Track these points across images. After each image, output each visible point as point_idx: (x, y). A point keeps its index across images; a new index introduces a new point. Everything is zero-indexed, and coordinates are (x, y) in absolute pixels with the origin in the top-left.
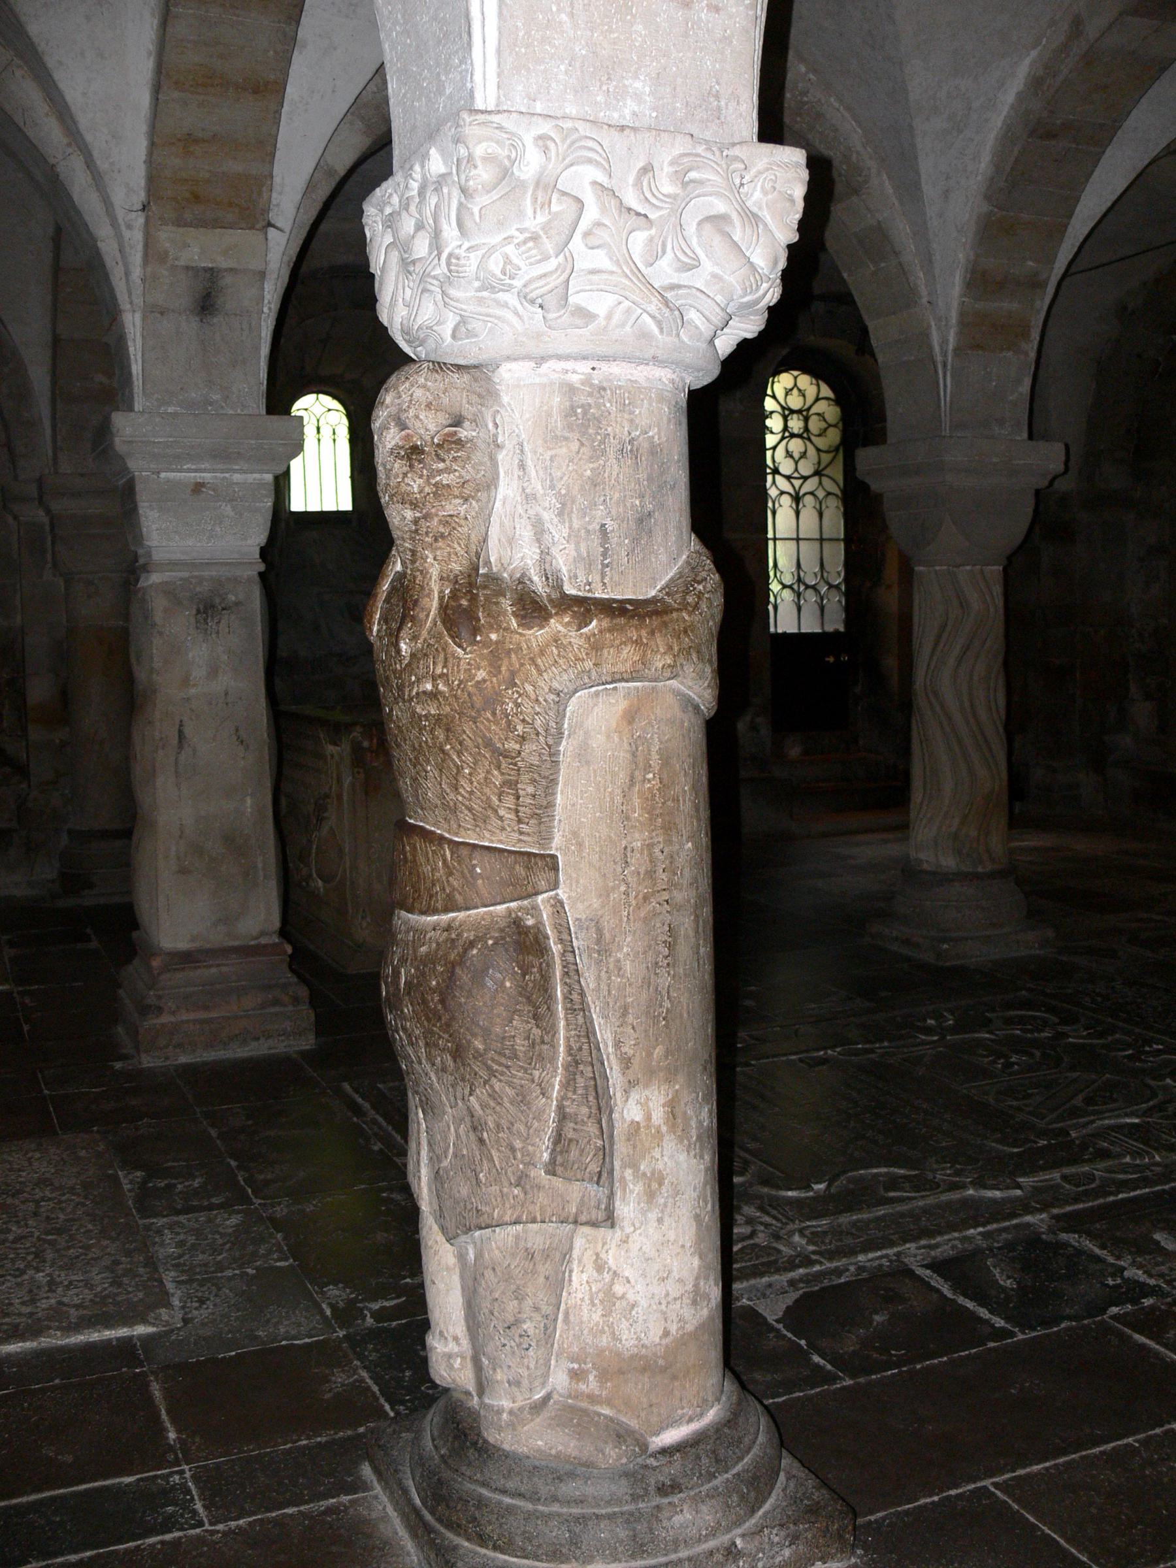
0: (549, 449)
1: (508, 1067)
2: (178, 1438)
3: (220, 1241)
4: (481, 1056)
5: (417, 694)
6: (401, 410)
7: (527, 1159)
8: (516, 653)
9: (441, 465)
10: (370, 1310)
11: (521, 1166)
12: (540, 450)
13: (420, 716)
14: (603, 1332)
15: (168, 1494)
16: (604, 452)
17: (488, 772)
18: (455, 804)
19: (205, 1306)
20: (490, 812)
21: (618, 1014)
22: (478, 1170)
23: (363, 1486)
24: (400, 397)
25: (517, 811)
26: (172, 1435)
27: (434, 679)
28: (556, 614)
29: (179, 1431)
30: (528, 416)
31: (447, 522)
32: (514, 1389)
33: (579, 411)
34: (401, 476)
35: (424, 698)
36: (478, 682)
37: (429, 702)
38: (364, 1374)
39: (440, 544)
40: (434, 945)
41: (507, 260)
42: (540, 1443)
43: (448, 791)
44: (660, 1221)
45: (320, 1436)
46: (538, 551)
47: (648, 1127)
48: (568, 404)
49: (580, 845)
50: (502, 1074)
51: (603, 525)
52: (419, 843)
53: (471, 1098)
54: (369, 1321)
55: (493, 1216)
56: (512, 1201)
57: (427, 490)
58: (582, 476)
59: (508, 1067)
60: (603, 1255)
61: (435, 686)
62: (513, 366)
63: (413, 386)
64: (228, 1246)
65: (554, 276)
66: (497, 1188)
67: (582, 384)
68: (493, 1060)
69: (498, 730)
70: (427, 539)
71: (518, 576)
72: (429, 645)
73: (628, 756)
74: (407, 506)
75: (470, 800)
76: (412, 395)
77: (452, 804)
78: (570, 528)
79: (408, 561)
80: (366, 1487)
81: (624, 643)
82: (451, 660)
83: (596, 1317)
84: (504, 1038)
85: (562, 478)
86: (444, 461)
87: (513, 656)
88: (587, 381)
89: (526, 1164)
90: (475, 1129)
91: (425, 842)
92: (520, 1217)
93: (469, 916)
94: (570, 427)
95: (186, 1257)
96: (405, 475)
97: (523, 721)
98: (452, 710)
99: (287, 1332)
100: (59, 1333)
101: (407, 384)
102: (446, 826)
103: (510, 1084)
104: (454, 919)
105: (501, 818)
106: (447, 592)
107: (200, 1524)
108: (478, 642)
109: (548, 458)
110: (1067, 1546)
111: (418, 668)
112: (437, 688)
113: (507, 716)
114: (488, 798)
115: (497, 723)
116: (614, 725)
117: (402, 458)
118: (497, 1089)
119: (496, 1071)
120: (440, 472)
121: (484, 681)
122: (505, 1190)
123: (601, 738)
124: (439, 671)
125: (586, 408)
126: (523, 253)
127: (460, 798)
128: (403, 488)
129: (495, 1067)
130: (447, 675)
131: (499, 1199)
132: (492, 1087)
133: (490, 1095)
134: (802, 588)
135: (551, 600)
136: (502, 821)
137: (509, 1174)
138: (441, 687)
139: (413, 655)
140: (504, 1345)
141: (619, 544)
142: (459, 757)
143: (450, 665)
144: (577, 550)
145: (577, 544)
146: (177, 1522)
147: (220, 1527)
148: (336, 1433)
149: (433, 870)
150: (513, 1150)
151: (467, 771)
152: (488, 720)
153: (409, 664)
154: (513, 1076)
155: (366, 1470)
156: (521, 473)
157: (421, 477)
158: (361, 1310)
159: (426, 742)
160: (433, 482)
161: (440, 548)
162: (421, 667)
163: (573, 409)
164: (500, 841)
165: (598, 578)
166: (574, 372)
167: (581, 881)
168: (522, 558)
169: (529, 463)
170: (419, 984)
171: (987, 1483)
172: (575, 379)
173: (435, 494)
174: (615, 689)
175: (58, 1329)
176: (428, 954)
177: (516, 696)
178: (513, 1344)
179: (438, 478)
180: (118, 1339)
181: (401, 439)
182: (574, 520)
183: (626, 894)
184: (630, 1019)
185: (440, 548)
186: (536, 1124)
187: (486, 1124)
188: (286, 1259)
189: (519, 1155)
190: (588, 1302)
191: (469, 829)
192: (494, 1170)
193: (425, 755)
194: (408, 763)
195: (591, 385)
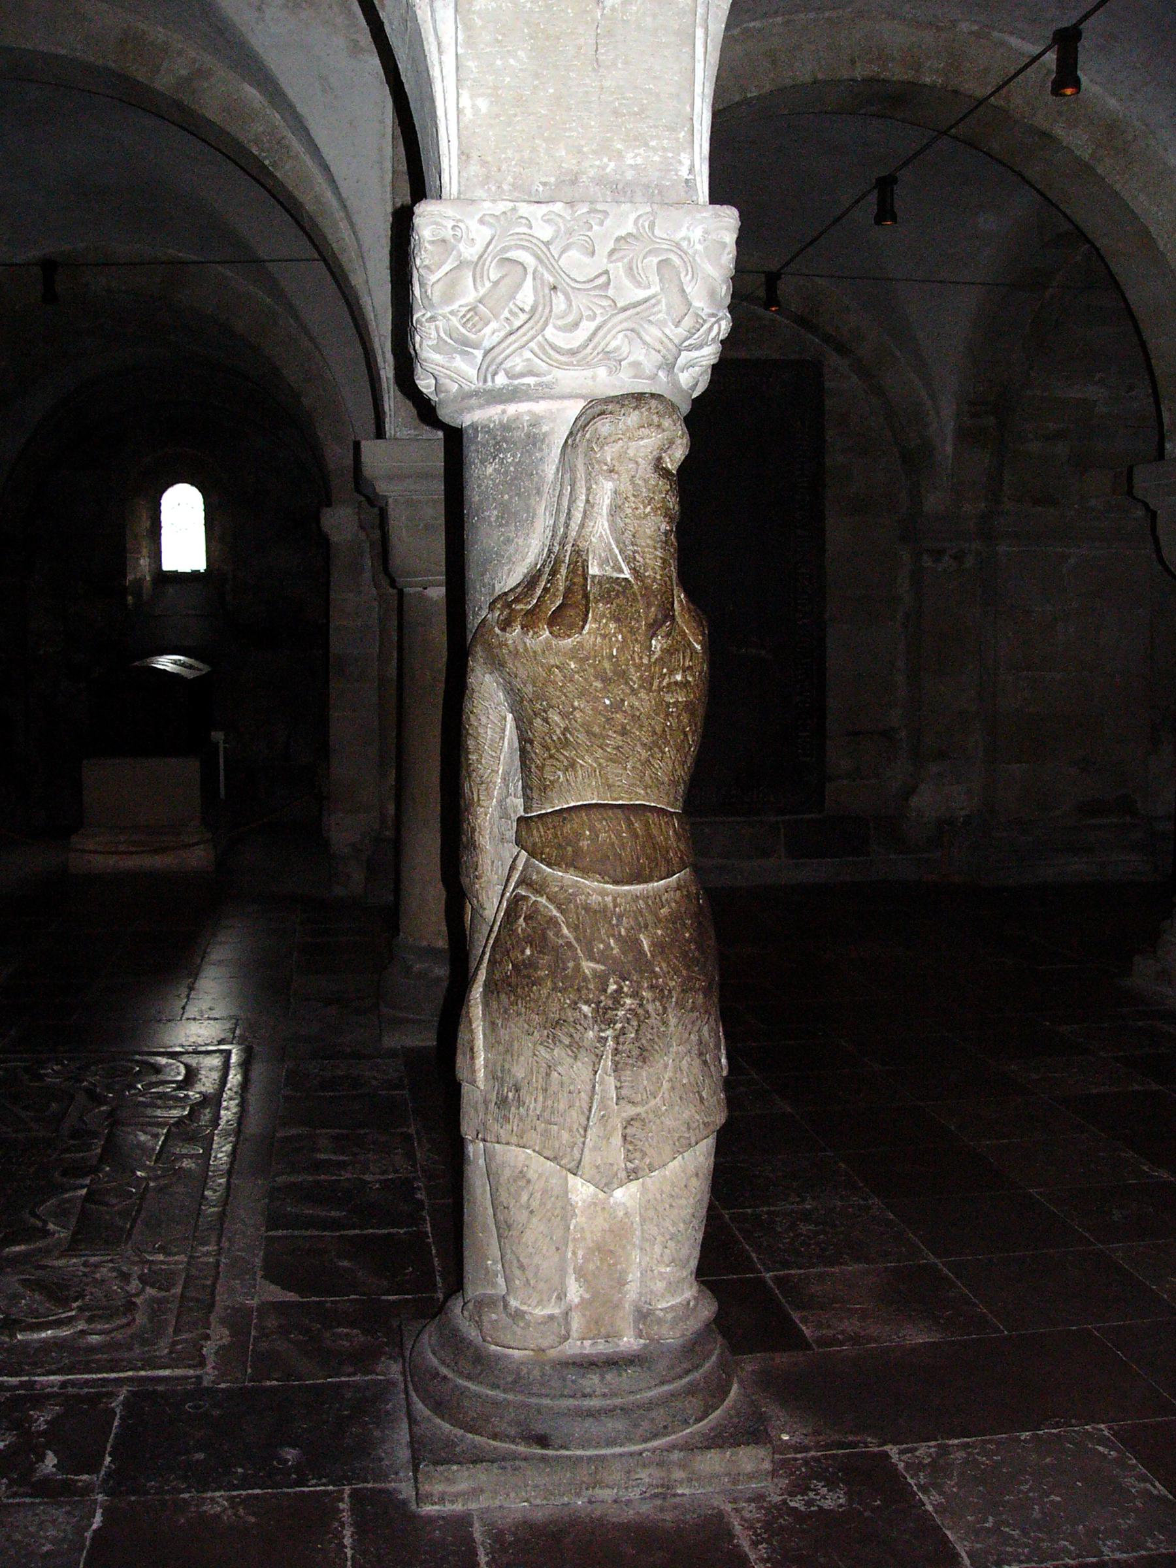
5: (669, 684)
13: (668, 705)
35: (674, 688)
40: (673, 904)
61: (684, 677)
124: (687, 664)
176: (671, 914)
194: (639, 748)
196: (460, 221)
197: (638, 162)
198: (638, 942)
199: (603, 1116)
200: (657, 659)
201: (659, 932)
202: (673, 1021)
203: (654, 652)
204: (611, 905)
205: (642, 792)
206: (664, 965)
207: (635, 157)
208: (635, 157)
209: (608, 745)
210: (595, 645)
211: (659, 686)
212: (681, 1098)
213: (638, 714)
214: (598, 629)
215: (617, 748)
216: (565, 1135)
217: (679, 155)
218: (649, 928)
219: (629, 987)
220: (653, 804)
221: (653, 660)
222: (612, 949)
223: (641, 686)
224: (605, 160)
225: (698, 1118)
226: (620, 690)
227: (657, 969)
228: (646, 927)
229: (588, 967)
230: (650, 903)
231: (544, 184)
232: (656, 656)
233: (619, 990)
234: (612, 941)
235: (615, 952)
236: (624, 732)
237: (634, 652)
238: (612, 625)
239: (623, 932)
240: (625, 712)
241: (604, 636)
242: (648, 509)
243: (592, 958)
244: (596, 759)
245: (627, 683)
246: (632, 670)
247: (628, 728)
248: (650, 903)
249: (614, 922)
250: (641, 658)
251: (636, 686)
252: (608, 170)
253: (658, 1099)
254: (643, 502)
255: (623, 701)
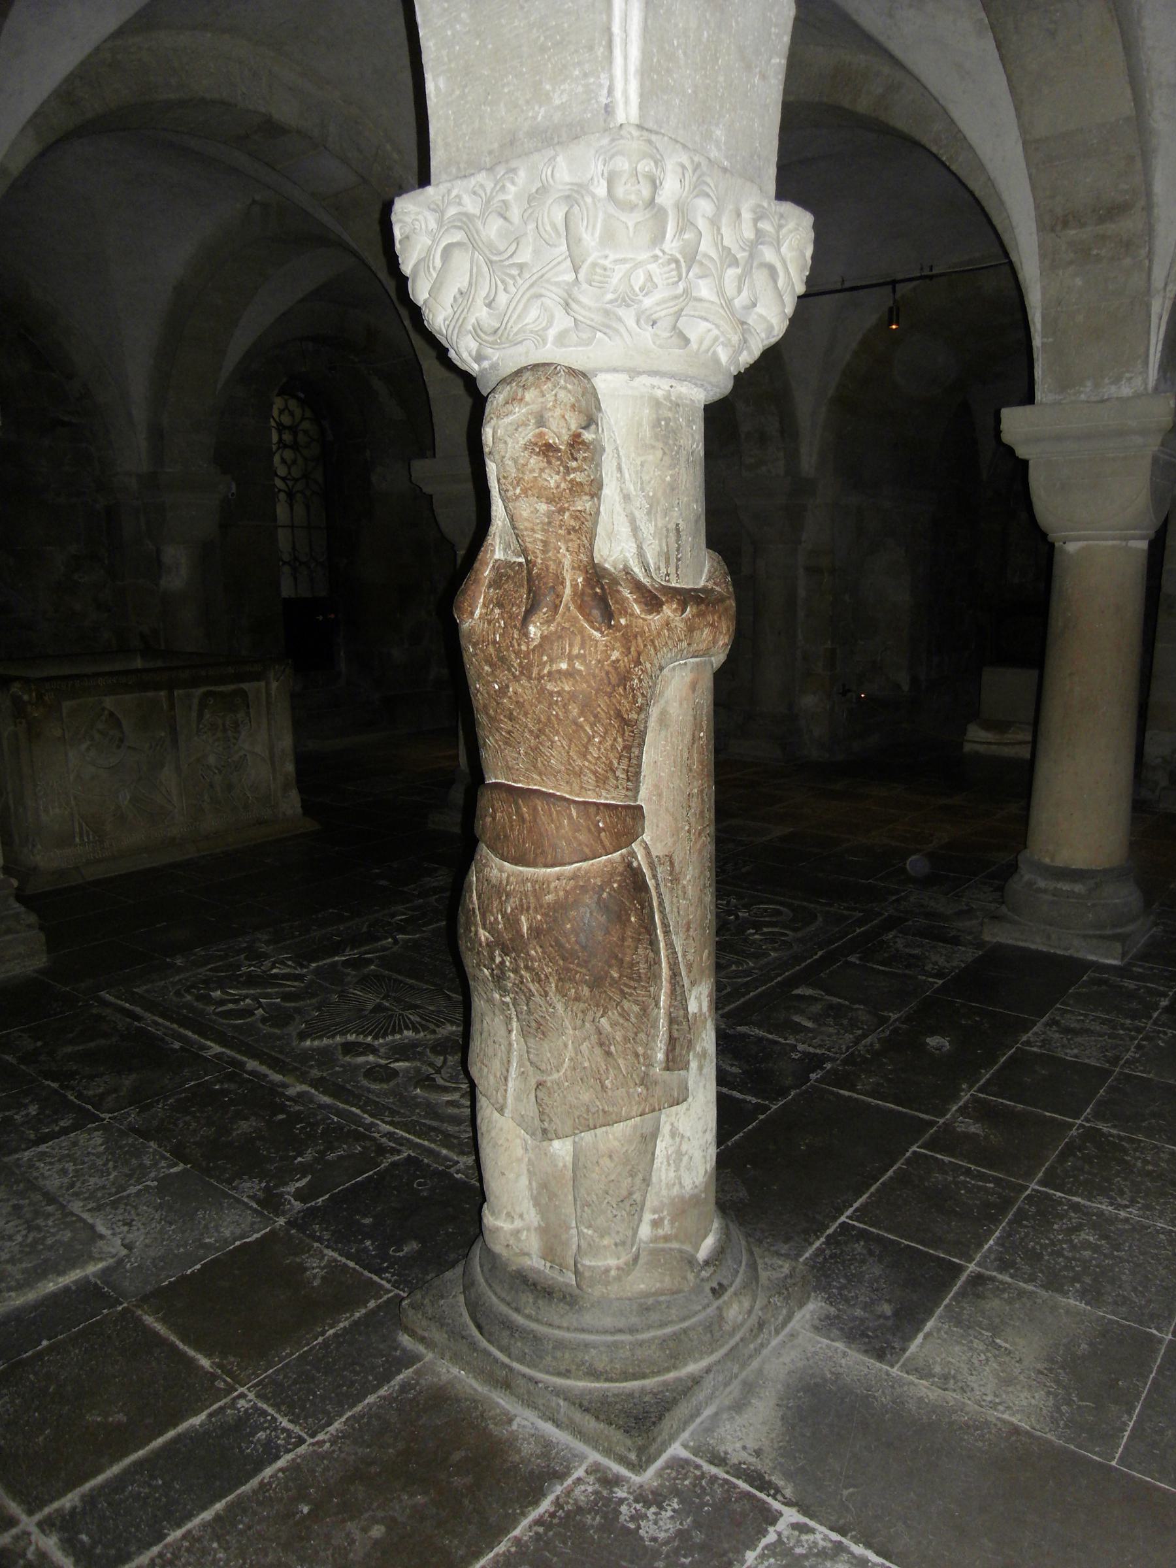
0: (639, 455)
1: (635, 988)
2: (213, 1363)
3: (99, 1162)
4: (616, 982)
5: (550, 673)
6: (544, 408)
7: (647, 1062)
8: (641, 637)
9: (574, 464)
10: (289, 1193)
11: (643, 1068)
12: (633, 455)
13: (551, 694)
14: (674, 1184)
15: (242, 1425)
16: (679, 460)
17: (615, 740)
18: (581, 769)
19: (135, 1228)
20: (610, 775)
21: (684, 930)
22: (604, 1077)
23: (410, 1359)
24: (544, 396)
25: (628, 772)
26: (205, 1362)
27: (571, 659)
28: (667, 601)
29: (209, 1356)
30: (622, 424)
31: (577, 516)
32: (620, 1248)
33: (663, 423)
34: (537, 471)
35: (557, 676)
36: (613, 662)
37: (564, 680)
38: (330, 1253)
39: (572, 537)
41: (650, 277)
42: (642, 1286)
43: (575, 757)
44: (705, 1087)
45: (340, 1322)
46: (634, 545)
47: (700, 1016)
48: (654, 416)
49: (660, 795)
50: (631, 995)
51: (677, 525)
52: (540, 805)
53: (602, 1019)
54: (298, 1205)
55: (621, 1113)
56: (637, 1098)
57: (563, 485)
58: (664, 481)
59: (635, 988)
60: (675, 1124)
62: (609, 377)
63: (555, 386)
64: (111, 1164)
65: (682, 299)
66: (624, 1090)
67: (665, 399)
68: (626, 985)
69: (626, 704)
70: (560, 531)
71: (621, 566)
72: (563, 628)
73: (692, 719)
74: (543, 500)
75: (596, 764)
76: (556, 395)
77: (577, 768)
78: (656, 526)
79: (538, 551)
80: (417, 1358)
81: (705, 626)
82: (588, 642)
83: (672, 1174)
84: (632, 965)
85: (649, 482)
86: (576, 459)
87: (639, 638)
88: (668, 397)
89: (647, 1066)
90: (601, 1044)
91: (547, 804)
92: (644, 1110)
93: (592, 865)
94: (656, 437)
95: (78, 1184)
96: (542, 470)
97: (642, 694)
98: (588, 687)
99: (232, 1233)
100: (13, 1294)
101: (549, 385)
102: (568, 788)
103: (636, 1002)
104: (579, 869)
105: (617, 778)
106: (580, 580)
107: (302, 1442)
108: (614, 626)
109: (639, 463)
110: (926, 1249)
111: (552, 649)
112: (574, 667)
113: (633, 690)
114: (611, 762)
115: (626, 697)
116: (684, 695)
117: (538, 454)
118: (626, 1008)
119: (627, 993)
120: (575, 470)
121: (618, 661)
122: (631, 1090)
123: (676, 704)
124: (576, 651)
125: (668, 420)
126: (665, 273)
127: (586, 764)
128: (541, 482)
129: (626, 990)
130: (584, 656)
131: (625, 1099)
132: (622, 1008)
133: (620, 1014)
134: (297, 564)
135: (656, 589)
136: (617, 781)
137: (634, 1076)
138: (578, 666)
139: (543, 637)
140: (615, 1216)
141: (686, 541)
142: (592, 728)
143: (587, 647)
144: (660, 546)
145: (660, 540)
146: (278, 1447)
147: (321, 1437)
148: (352, 1315)
149: (557, 828)
150: (637, 1055)
151: (597, 740)
152: (620, 695)
153: (540, 645)
154: (638, 995)
155: (405, 1340)
156: (619, 475)
157: (558, 473)
158: (281, 1195)
159: (557, 716)
160: (568, 478)
161: (572, 540)
162: (555, 648)
163: (659, 420)
164: (613, 798)
165: (674, 570)
166: (659, 388)
167: (660, 825)
168: (621, 552)
169: (624, 466)
170: (550, 929)
171: (843, 1219)
172: (659, 393)
173: (571, 490)
174: (686, 663)
175: (10, 1289)
176: (556, 902)
177: (640, 673)
178: (624, 1213)
179: (572, 476)
180: (75, 1282)
181: (535, 436)
182: (659, 519)
183: (689, 831)
184: (691, 933)
185: (572, 540)
186: (652, 1031)
187: (614, 1039)
188: (176, 1165)
189: (642, 1059)
190: (665, 1163)
191: (589, 790)
192: (621, 1076)
193: (553, 727)
194: (527, 735)
195: (671, 401)
196: (418, 214)
197: (564, 100)
198: (518, 921)
199: (523, 1073)
200: (535, 646)
201: (539, 917)
202: (560, 1007)
203: (533, 639)
204: (504, 882)
205: (538, 778)
206: (539, 950)
207: (561, 94)
208: (561, 94)
209: (502, 728)
210: (483, 630)
211: (539, 674)
212: (581, 1079)
213: (521, 700)
214: (486, 614)
215: (509, 732)
216: (491, 1078)
217: (599, 77)
218: (531, 912)
219: (511, 963)
220: (551, 791)
221: (531, 647)
222: (498, 923)
223: (522, 673)
224: (537, 108)
225: (598, 1103)
226: (504, 675)
227: (533, 952)
228: (528, 908)
229: (483, 935)
230: (537, 887)
231: (490, 152)
232: (535, 643)
233: (503, 962)
234: (500, 917)
235: (500, 927)
236: (511, 718)
237: (513, 638)
238: (497, 611)
239: (509, 910)
240: (510, 698)
241: (489, 622)
242: (518, 491)
243: (484, 928)
244: (496, 741)
245: (509, 670)
246: (513, 656)
247: (515, 714)
248: (537, 887)
249: (504, 898)
250: (519, 645)
251: (517, 673)
252: (540, 118)
253: (561, 1073)
254: (511, 484)
255: (507, 687)
